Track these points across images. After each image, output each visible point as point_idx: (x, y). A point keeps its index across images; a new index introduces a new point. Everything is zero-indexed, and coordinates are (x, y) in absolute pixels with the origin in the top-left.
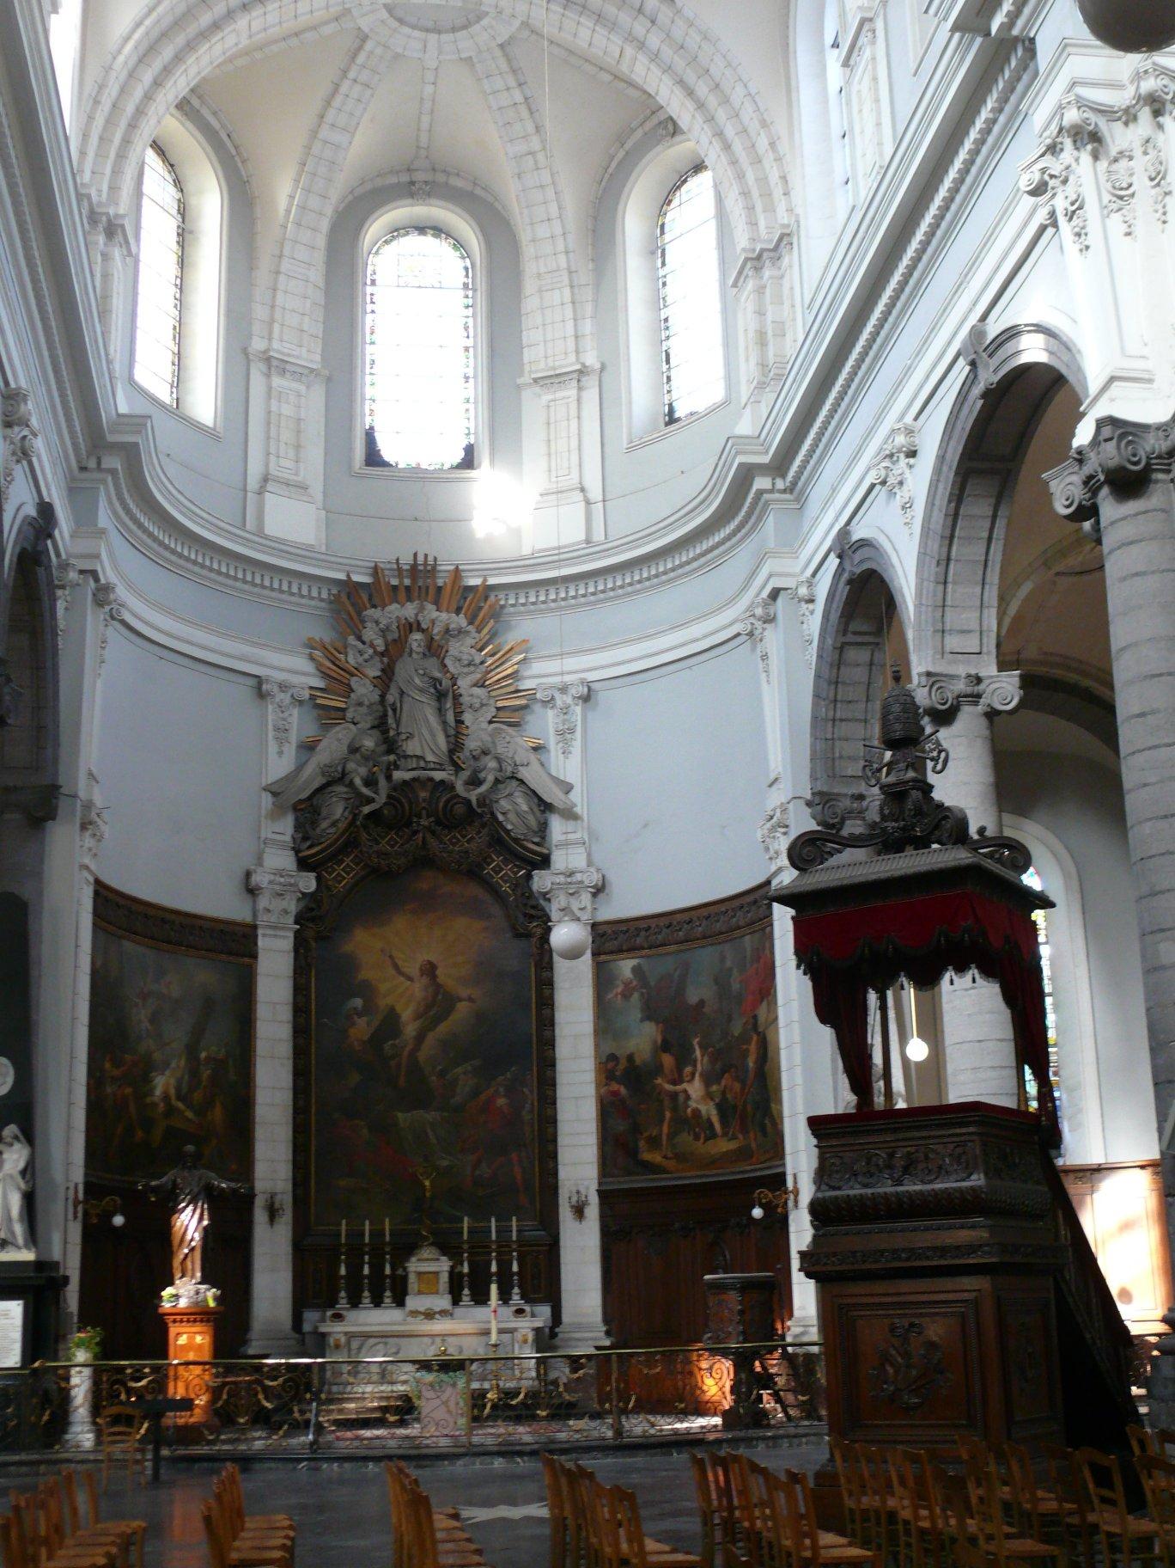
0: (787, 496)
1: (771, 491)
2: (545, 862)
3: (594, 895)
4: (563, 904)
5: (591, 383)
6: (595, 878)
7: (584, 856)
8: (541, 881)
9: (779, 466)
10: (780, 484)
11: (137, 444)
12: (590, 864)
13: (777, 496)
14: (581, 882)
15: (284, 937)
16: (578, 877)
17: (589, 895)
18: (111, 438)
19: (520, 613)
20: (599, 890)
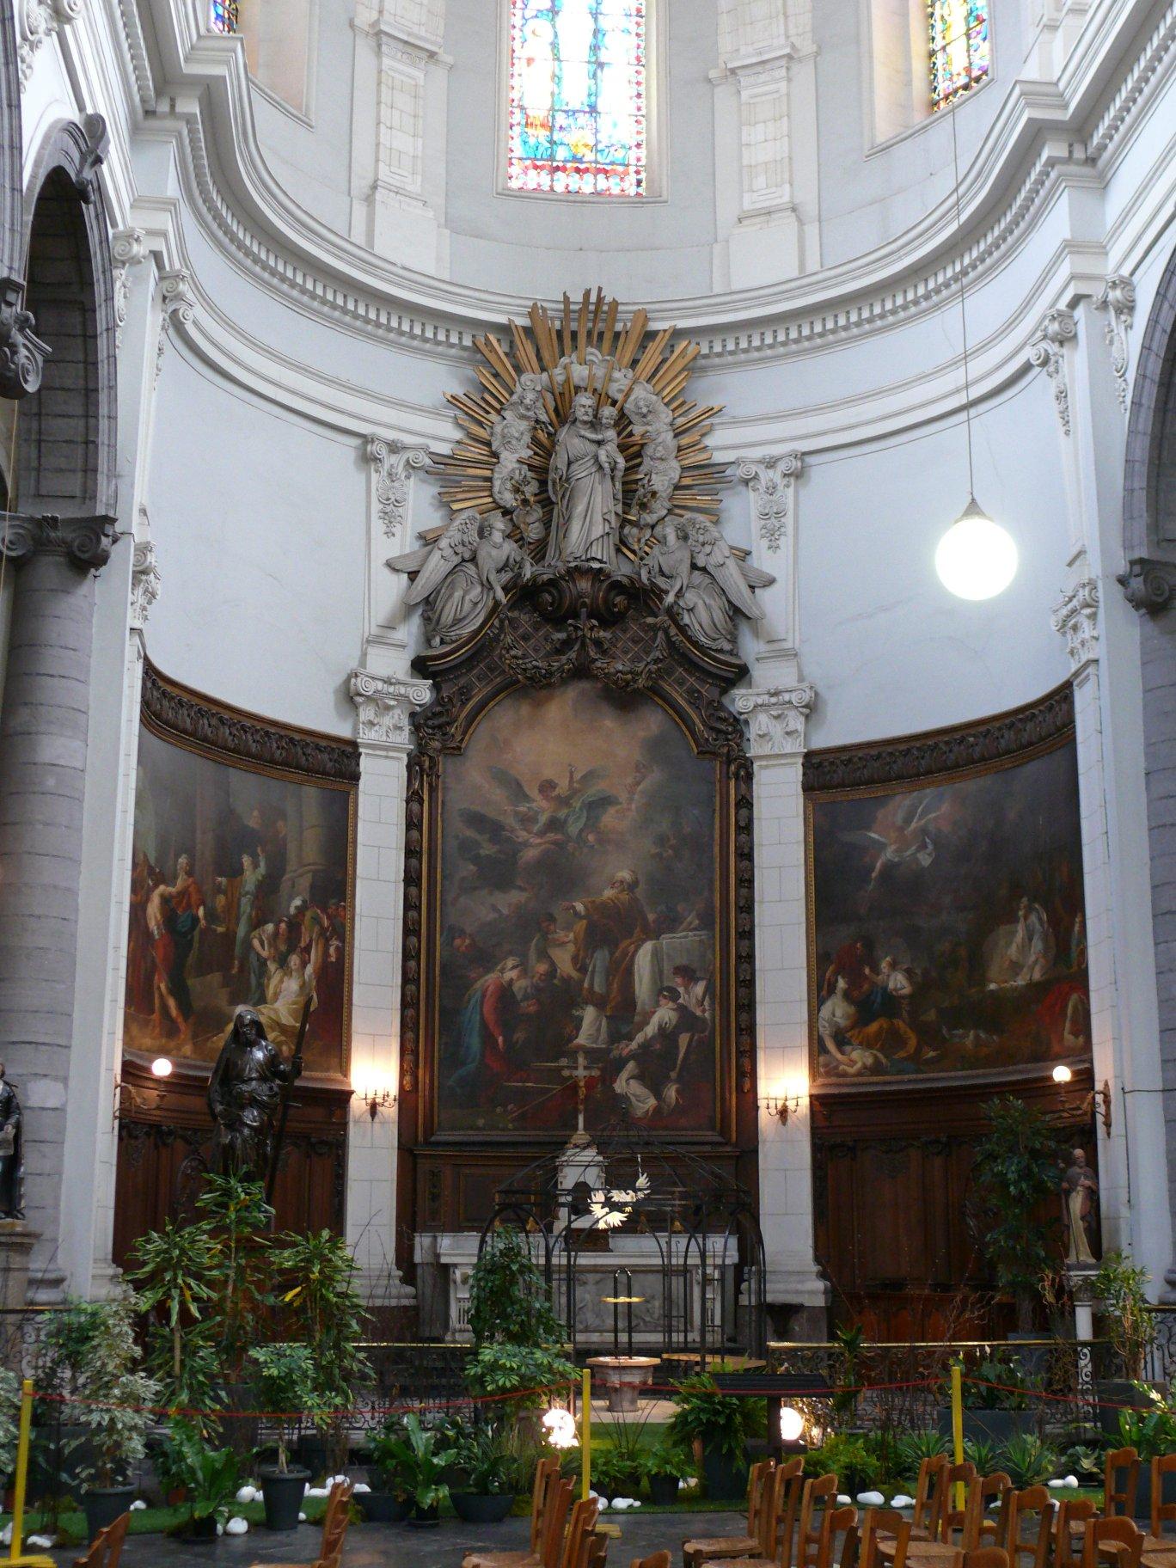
0: (1086, 170)
1: (1070, 159)
2: (740, 674)
3: (807, 717)
4: (764, 728)
5: (804, 74)
6: (807, 697)
7: (795, 670)
8: (741, 700)
9: (1081, 127)
10: (1079, 154)
11: (224, 78)
12: (801, 679)
13: (1073, 169)
14: (790, 702)
15: (398, 759)
16: (787, 697)
17: (802, 719)
18: (188, 69)
19: (714, 367)
20: (811, 710)
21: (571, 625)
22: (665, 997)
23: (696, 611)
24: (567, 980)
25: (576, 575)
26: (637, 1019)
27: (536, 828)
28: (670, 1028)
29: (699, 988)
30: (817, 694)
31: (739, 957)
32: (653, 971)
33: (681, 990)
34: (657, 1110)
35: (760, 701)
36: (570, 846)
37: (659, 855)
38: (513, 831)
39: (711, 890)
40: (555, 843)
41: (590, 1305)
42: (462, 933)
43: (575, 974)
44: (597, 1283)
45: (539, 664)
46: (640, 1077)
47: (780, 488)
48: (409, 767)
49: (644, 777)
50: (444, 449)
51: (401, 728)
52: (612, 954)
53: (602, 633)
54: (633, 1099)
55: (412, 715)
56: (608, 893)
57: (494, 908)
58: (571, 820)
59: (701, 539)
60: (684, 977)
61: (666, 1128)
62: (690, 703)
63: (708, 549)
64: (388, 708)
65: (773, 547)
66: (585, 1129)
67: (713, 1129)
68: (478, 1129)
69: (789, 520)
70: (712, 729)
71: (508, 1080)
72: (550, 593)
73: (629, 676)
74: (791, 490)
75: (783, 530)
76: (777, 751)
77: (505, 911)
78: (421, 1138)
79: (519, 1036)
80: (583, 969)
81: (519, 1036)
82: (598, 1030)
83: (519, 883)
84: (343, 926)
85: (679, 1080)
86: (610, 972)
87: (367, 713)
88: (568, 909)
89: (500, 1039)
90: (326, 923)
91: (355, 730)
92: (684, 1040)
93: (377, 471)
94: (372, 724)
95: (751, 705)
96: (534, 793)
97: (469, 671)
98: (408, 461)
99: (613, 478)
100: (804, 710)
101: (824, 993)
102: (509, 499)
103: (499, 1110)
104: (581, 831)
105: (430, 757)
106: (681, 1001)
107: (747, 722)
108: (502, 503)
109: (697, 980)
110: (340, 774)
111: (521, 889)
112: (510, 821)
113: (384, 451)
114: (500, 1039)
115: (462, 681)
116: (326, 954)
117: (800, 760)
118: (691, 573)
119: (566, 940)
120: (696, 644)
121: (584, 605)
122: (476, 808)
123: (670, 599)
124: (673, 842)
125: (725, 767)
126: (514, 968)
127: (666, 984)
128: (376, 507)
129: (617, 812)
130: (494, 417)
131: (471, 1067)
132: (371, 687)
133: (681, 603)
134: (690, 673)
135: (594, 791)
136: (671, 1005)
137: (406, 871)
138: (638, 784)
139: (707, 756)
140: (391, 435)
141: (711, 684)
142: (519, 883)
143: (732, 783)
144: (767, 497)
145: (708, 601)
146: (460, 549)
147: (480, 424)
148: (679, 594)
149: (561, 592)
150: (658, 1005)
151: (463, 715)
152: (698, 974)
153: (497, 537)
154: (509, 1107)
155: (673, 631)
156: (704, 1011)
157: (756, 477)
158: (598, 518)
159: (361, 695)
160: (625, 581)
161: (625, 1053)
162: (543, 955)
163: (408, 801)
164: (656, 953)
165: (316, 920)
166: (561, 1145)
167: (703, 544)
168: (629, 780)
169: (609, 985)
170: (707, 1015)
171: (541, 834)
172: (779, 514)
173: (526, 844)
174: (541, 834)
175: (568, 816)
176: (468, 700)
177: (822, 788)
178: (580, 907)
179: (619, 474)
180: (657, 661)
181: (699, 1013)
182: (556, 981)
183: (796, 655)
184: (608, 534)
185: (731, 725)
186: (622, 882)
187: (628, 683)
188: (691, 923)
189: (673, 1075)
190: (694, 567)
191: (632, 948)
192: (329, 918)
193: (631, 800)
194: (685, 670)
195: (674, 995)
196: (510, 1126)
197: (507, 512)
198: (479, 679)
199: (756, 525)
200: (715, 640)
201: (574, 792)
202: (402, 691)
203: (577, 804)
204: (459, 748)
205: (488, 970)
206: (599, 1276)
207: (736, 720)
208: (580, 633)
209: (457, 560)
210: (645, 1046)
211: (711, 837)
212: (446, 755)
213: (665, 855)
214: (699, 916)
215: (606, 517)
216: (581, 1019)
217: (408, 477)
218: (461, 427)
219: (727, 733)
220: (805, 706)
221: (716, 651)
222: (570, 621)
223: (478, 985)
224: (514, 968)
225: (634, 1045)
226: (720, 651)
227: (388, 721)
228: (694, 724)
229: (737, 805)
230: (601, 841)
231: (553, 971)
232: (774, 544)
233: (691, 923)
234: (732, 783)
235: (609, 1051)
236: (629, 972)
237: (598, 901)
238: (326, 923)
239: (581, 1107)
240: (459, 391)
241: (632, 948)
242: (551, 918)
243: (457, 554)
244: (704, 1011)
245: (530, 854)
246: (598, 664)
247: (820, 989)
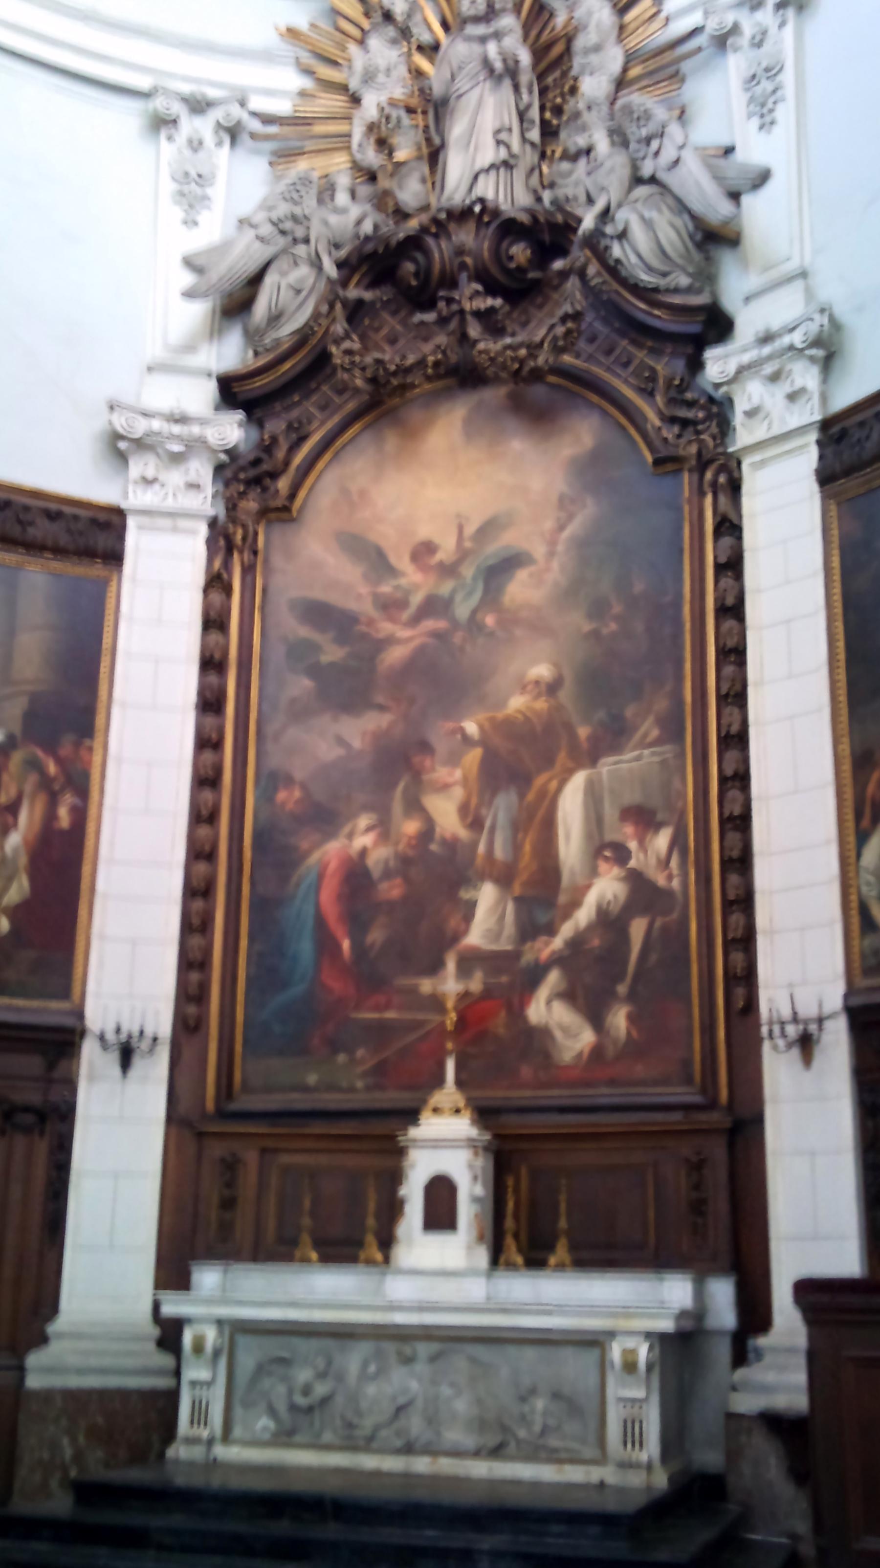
4: (756, 401)
14: (791, 348)
16: (786, 340)
21: (442, 298)
22: (607, 859)
23: (630, 235)
24: (451, 845)
25: (452, 227)
26: (562, 899)
27: (406, 615)
28: (615, 909)
29: (662, 840)
30: (832, 320)
31: (723, 780)
32: (587, 818)
33: (633, 845)
34: (597, 1052)
35: (746, 358)
36: (458, 638)
37: (595, 634)
38: (371, 622)
39: (679, 679)
40: (437, 635)
41: (419, 1403)
42: (289, 781)
43: (463, 833)
44: (433, 1359)
45: (387, 357)
46: (568, 995)
47: (773, 30)
48: (211, 543)
49: (571, 517)
50: (283, 107)
51: (194, 486)
52: (522, 796)
53: (490, 302)
54: (558, 1034)
55: (219, 469)
56: (517, 703)
57: (340, 741)
58: (459, 598)
59: (644, 132)
60: (636, 824)
61: (612, 1082)
62: (641, 391)
63: (655, 144)
64: (177, 459)
65: (767, 124)
66: (460, 1083)
67: (688, 1080)
68: (306, 1089)
69: (788, 78)
70: (673, 420)
71: (358, 1007)
72: (415, 261)
73: (523, 352)
74: (789, 31)
75: (779, 93)
76: (776, 430)
77: (357, 744)
78: (210, 1105)
79: (376, 936)
80: (476, 824)
81: (376, 936)
82: (502, 917)
83: (380, 699)
84: (86, 776)
85: (632, 997)
86: (517, 827)
87: (138, 466)
88: (453, 732)
89: (346, 944)
90: (52, 768)
91: (126, 495)
92: (638, 929)
93: (170, 138)
94: (148, 482)
95: (731, 367)
96: (402, 562)
97: (307, 396)
98: (219, 125)
99: (516, 88)
100: (813, 352)
101: (866, 822)
102: (371, 157)
103: (342, 1058)
104: (474, 612)
105: (244, 527)
106: (632, 863)
107: (730, 401)
108: (365, 164)
109: (657, 827)
110: (88, 554)
111: (382, 708)
112: (365, 607)
113: (177, 108)
114: (346, 944)
115: (295, 413)
116: (51, 815)
117: (813, 436)
118: (630, 190)
119: (450, 780)
120: (637, 290)
121: (463, 266)
122: (318, 594)
123: (588, 222)
124: (617, 609)
125: (696, 477)
126: (369, 829)
127: (610, 836)
128: (168, 187)
129: (531, 575)
130: (353, 49)
131: (297, 990)
132: (140, 427)
133: (609, 230)
134: (640, 346)
135: (494, 548)
136: (616, 871)
137: (201, 693)
138: (561, 528)
139: (670, 467)
140: (186, 88)
141: (673, 354)
142: (380, 699)
143: (709, 500)
144: (756, 52)
145: (647, 214)
146: (288, 225)
147: (334, 63)
148: (606, 215)
149: (427, 253)
150: (594, 873)
151: (299, 458)
152: (660, 817)
153: (342, 198)
154: (360, 1053)
155: (592, 269)
156: (670, 877)
157: (735, 29)
158: (490, 142)
159: (122, 437)
160: (524, 218)
161: (545, 954)
162: (414, 806)
163: (206, 590)
164: (593, 795)
165: (34, 765)
166: (411, 1116)
167: (648, 140)
168: (549, 525)
169: (516, 847)
170: (676, 884)
171: (416, 620)
172: (772, 71)
173: (390, 641)
174: (416, 620)
175: (454, 592)
176: (302, 439)
177: (849, 471)
178: (471, 727)
179: (526, 77)
180: (564, 319)
181: (661, 880)
182: (434, 847)
183: (803, 274)
184: (506, 164)
185: (703, 408)
186: (537, 683)
187: (522, 362)
188: (645, 735)
189: (622, 989)
190: (637, 180)
191: (554, 784)
192: (59, 761)
193: (551, 554)
194: (633, 342)
195: (621, 854)
196: (360, 1084)
197: (372, 177)
198: (323, 408)
199: (739, 99)
200: (665, 275)
201: (463, 555)
202: (196, 430)
203: (468, 571)
204: (286, 509)
205: (330, 835)
206: (435, 1347)
207: (711, 400)
208: (455, 307)
209: (281, 242)
210: (576, 943)
211: (679, 595)
212: (269, 522)
213: (605, 631)
214: (661, 722)
215: (503, 136)
216: (472, 906)
217: (219, 144)
218: (308, 72)
219: (694, 423)
220: (817, 343)
221: (668, 291)
222: (442, 293)
223: (314, 858)
224: (369, 829)
225: (558, 943)
226: (676, 290)
227: (175, 477)
228: (645, 419)
229: (718, 532)
230: (500, 622)
231: (428, 832)
232: (768, 119)
233: (645, 735)
234: (709, 500)
235: (513, 956)
236: (549, 825)
237: (500, 715)
238: (52, 768)
239: (450, 1045)
240: (302, 23)
241: (554, 784)
242: (425, 747)
243: (283, 233)
244: (670, 877)
245: (395, 655)
246: (481, 346)
247: (859, 815)
